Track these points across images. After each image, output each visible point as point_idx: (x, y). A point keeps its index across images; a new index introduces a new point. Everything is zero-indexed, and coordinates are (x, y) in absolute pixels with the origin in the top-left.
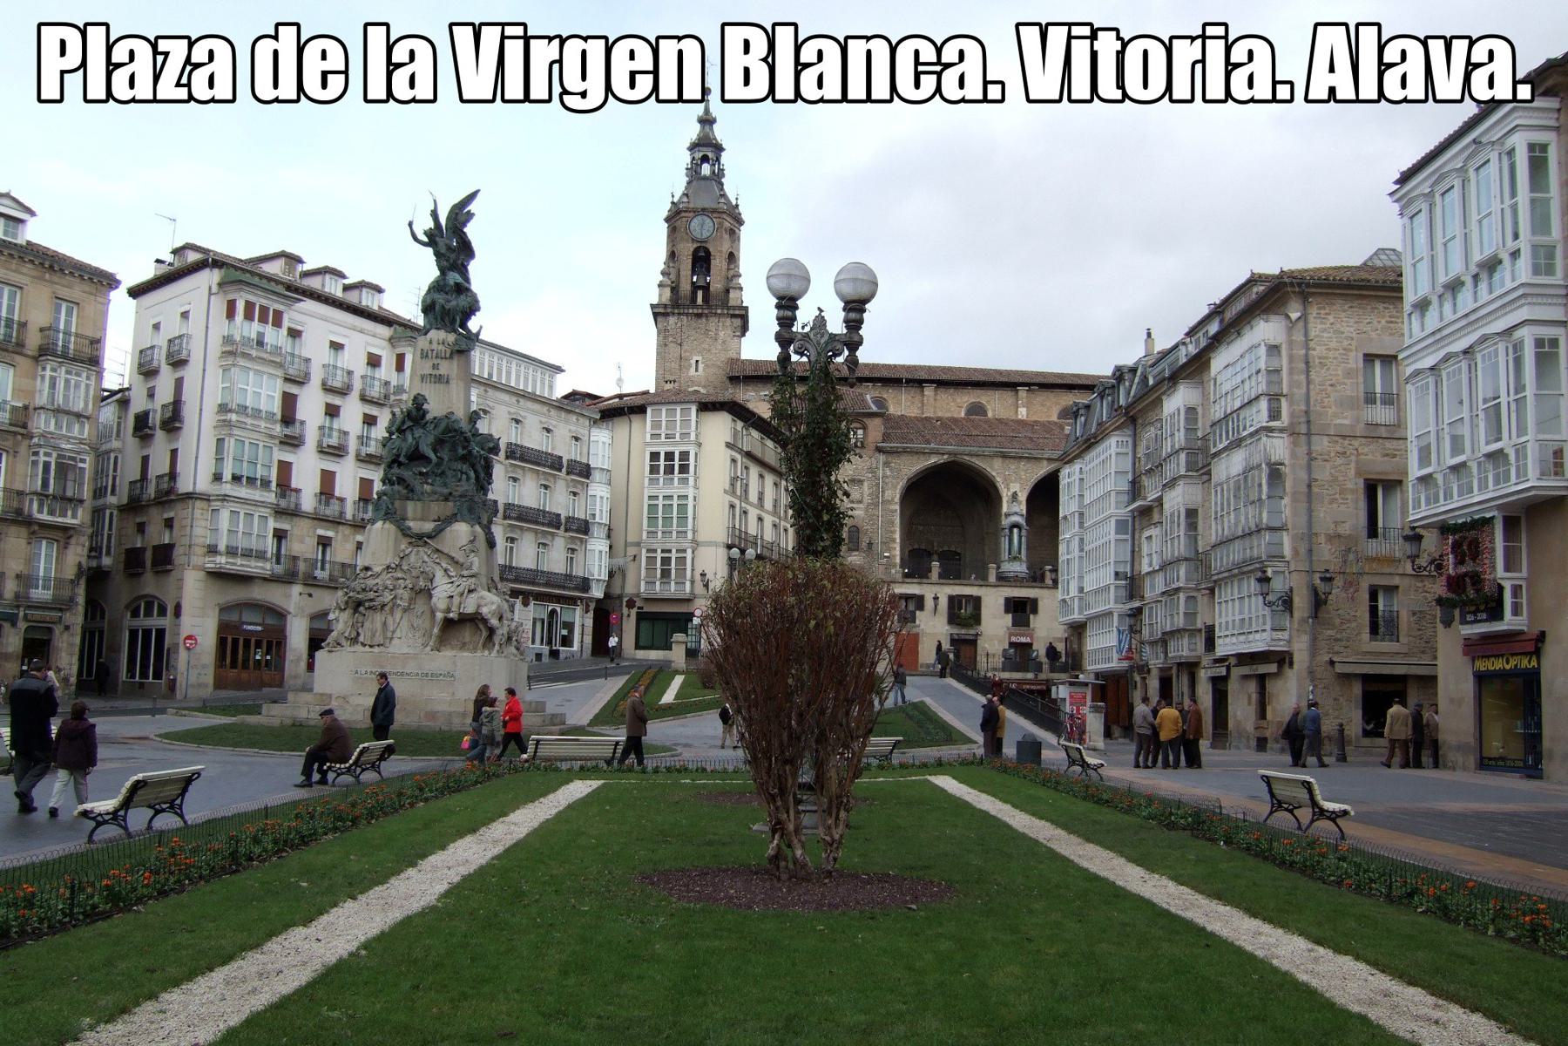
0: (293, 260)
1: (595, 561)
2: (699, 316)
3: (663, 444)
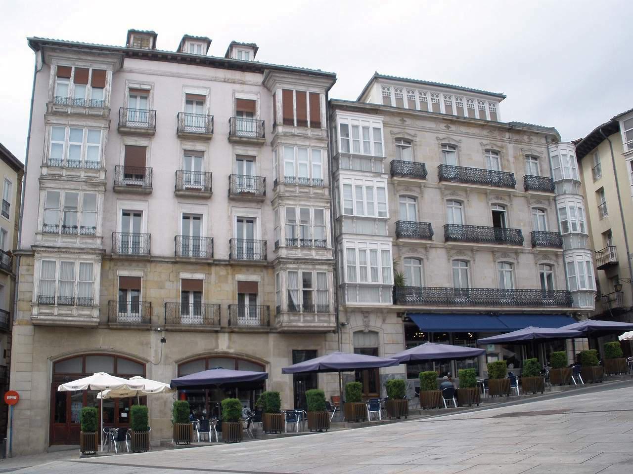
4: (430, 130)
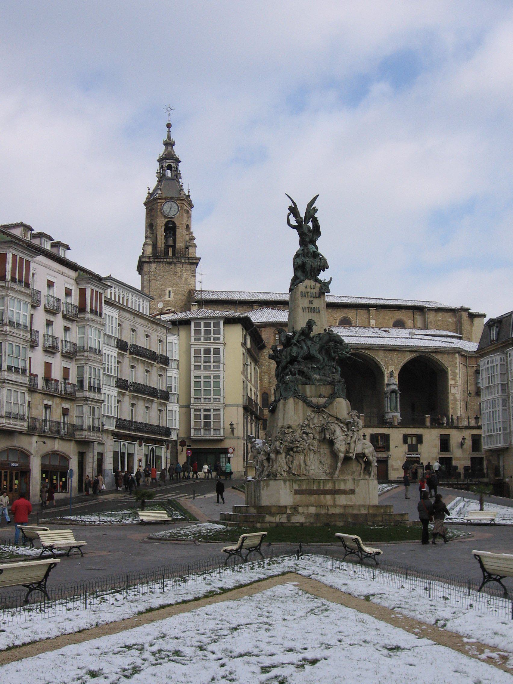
0: (28, 228)
1: (173, 417)
2: (170, 263)
3: (212, 343)
4: (129, 320)
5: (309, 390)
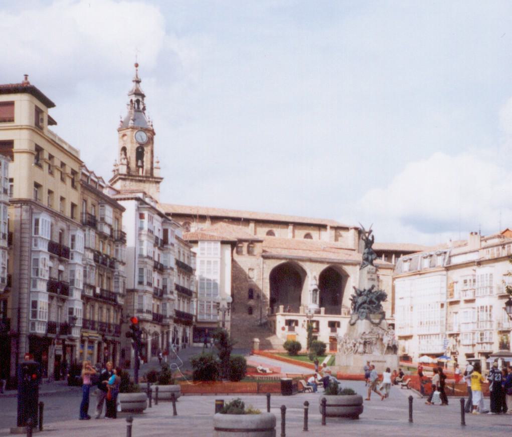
5: (371, 316)
